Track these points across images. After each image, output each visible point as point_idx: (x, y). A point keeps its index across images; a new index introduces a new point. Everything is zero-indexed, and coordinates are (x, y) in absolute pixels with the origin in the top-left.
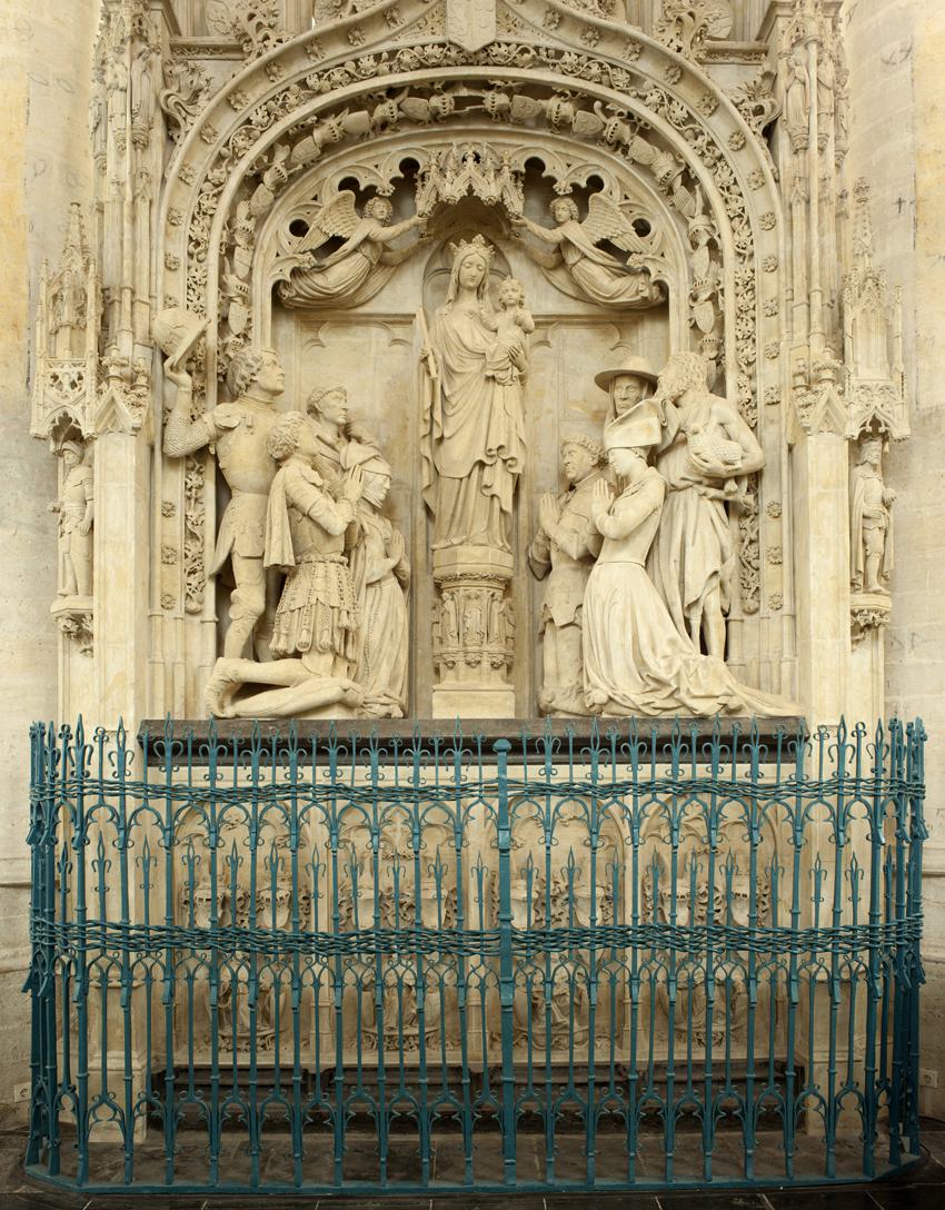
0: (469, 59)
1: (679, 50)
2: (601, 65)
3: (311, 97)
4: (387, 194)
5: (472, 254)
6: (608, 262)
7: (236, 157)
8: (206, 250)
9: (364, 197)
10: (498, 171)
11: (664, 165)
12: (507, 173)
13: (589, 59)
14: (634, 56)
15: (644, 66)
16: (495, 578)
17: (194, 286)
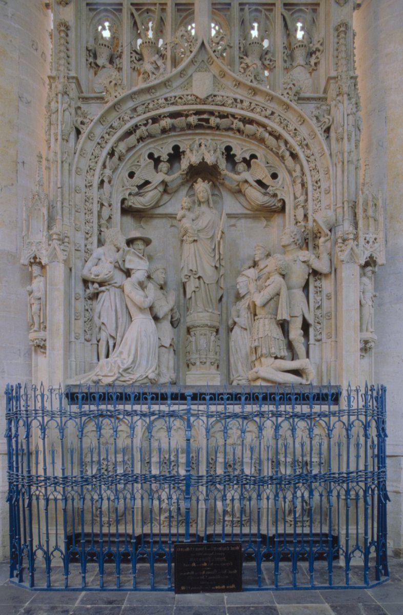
5: (202, 187)
9: (157, 161)
10: (215, 151)
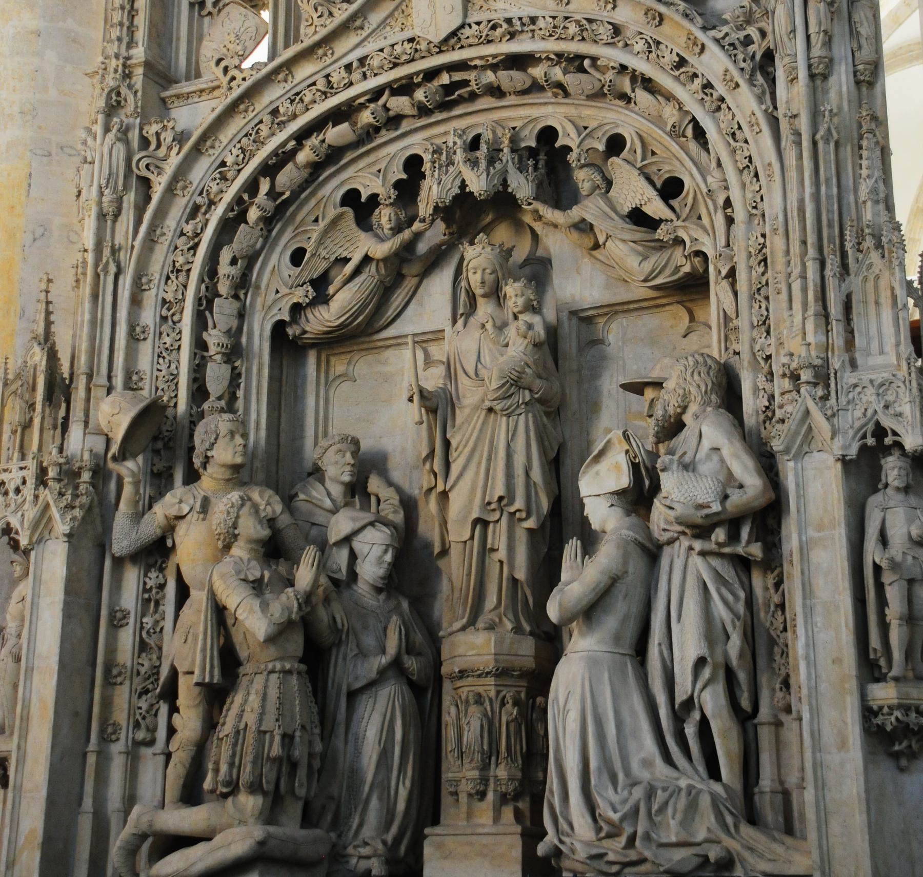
2: (578, 22)
7: (212, 203)
13: (566, 18)
17: (164, 354)
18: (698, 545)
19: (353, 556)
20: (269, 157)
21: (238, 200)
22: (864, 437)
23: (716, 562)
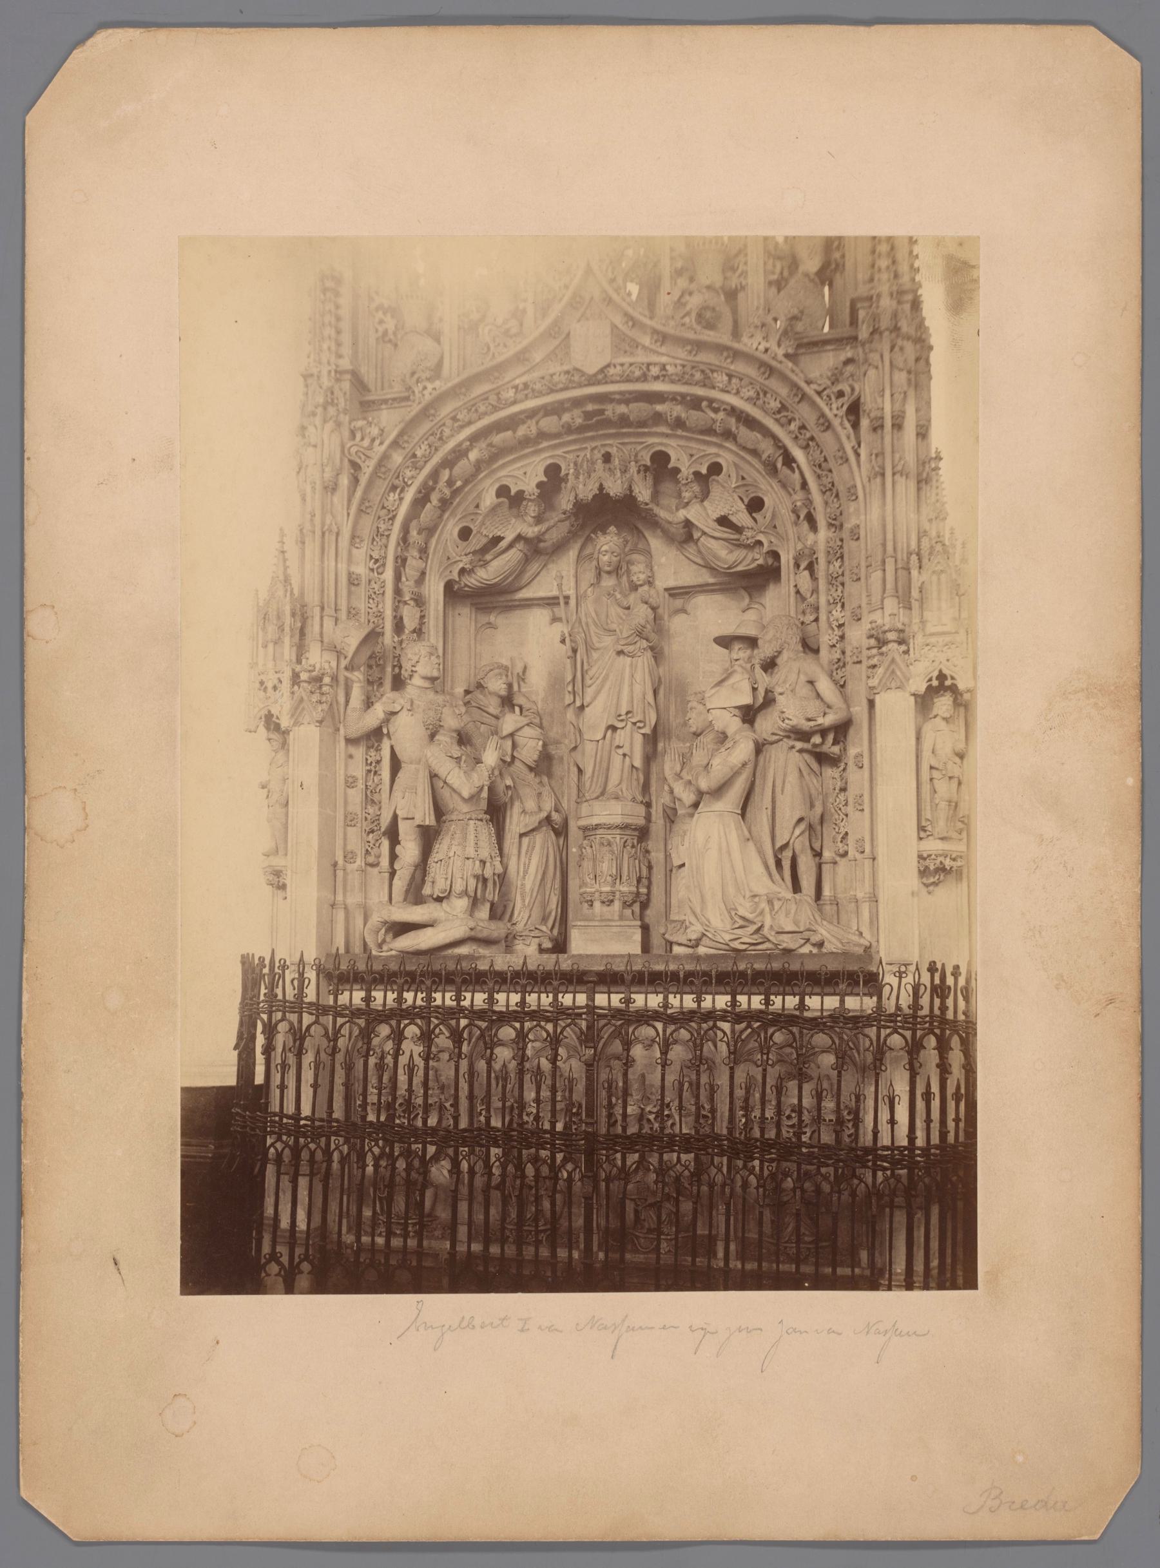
0: (592, 381)
1: (766, 350)
3: (462, 427)
4: (533, 497)
5: (608, 543)
6: (725, 536)
8: (384, 565)
11: (767, 448)
12: (633, 468)
14: (729, 360)
15: (740, 367)
16: (625, 827)
18: (799, 745)
19: (514, 746)
20: (450, 452)
21: (425, 483)
22: (930, 680)
23: (806, 756)
